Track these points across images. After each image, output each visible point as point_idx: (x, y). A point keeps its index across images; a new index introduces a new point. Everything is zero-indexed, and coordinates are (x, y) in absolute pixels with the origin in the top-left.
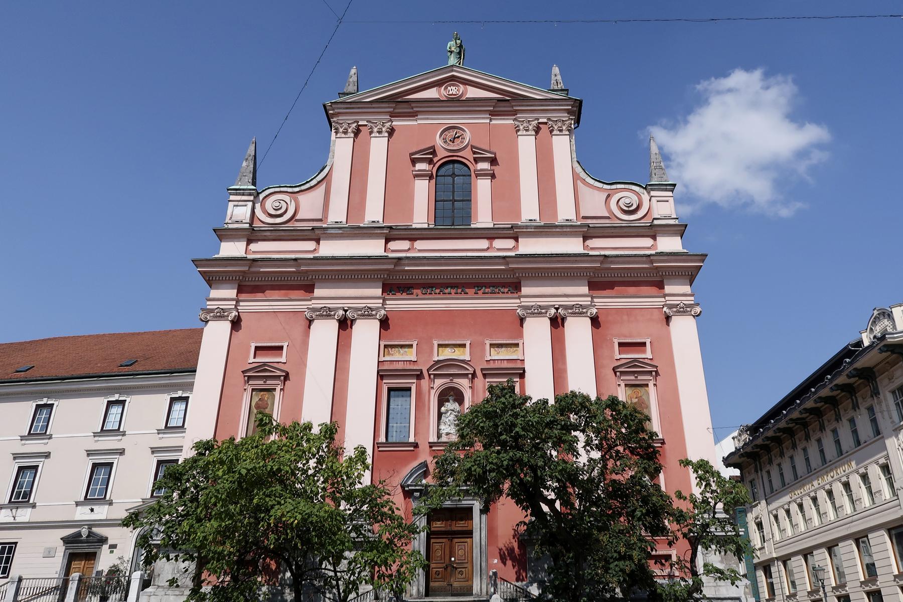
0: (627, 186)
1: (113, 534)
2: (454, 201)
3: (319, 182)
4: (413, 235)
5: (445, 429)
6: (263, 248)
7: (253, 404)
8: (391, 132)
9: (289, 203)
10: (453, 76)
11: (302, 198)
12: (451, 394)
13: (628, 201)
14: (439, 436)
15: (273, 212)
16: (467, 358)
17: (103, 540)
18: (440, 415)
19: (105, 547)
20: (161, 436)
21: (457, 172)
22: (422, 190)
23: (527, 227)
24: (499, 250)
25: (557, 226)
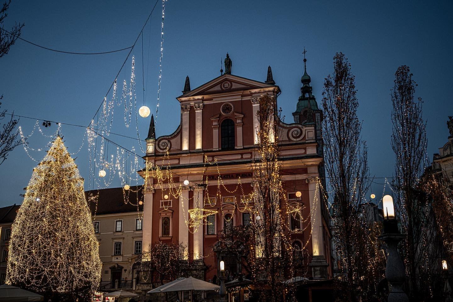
0: (296, 125)
1: (125, 267)
3: (178, 133)
7: (163, 223)
9: (167, 143)
10: (226, 78)
11: (172, 141)
13: (296, 132)
15: (162, 147)
17: (122, 268)
19: (123, 270)
20: (135, 233)
22: (216, 133)
24: (245, 159)
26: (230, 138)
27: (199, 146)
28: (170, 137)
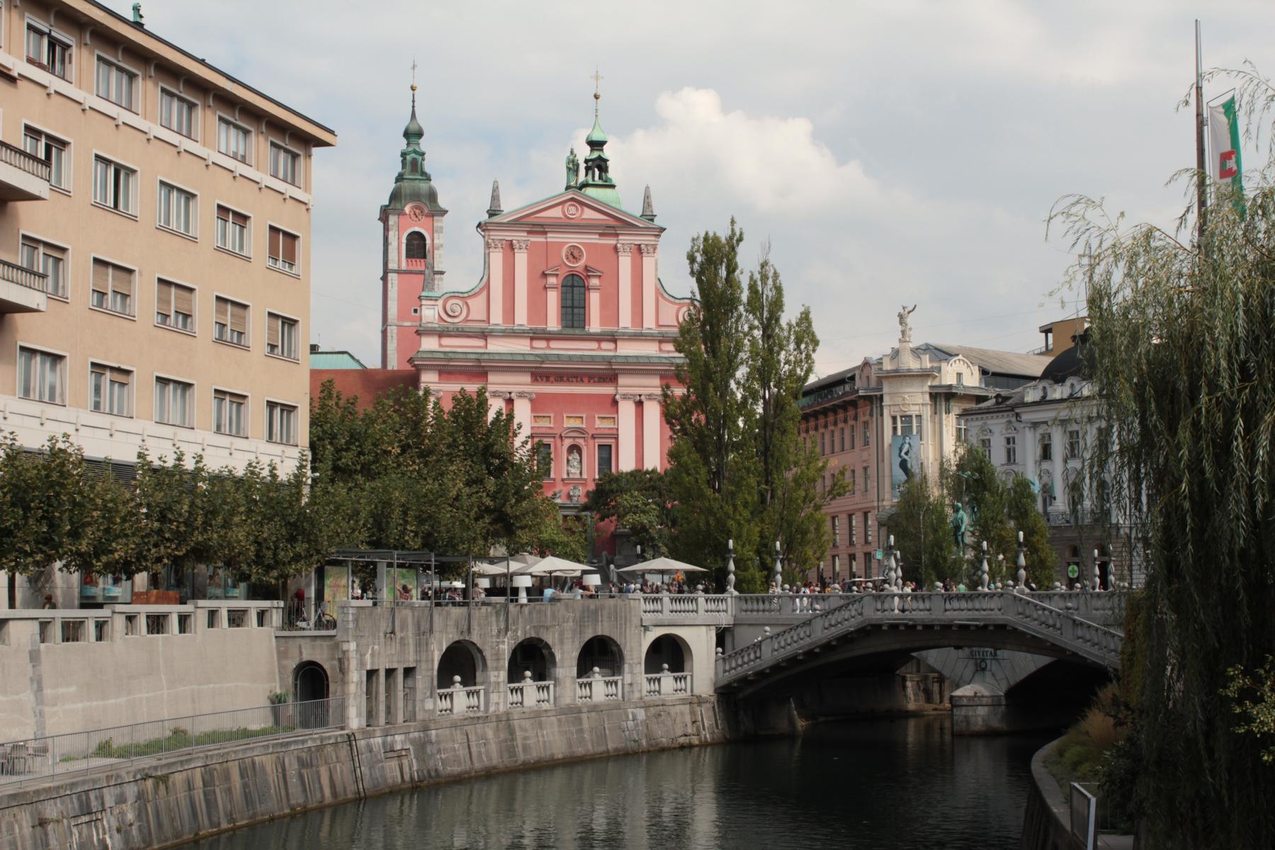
2: (573, 307)
3: (481, 290)
4: (548, 337)
5: (573, 470)
6: (451, 344)
8: (531, 249)
11: (469, 301)
12: (574, 448)
14: (568, 474)
15: (451, 313)
16: (584, 426)
18: (568, 461)
21: (576, 284)
22: (553, 298)
23: (624, 334)
25: (642, 335)
26: (576, 311)
27: (521, 319)
28: (466, 295)
